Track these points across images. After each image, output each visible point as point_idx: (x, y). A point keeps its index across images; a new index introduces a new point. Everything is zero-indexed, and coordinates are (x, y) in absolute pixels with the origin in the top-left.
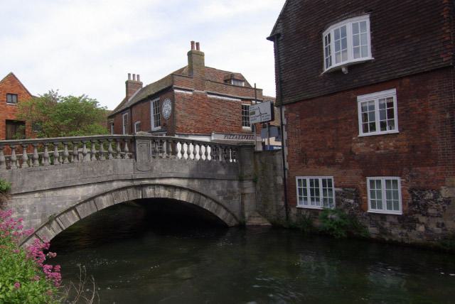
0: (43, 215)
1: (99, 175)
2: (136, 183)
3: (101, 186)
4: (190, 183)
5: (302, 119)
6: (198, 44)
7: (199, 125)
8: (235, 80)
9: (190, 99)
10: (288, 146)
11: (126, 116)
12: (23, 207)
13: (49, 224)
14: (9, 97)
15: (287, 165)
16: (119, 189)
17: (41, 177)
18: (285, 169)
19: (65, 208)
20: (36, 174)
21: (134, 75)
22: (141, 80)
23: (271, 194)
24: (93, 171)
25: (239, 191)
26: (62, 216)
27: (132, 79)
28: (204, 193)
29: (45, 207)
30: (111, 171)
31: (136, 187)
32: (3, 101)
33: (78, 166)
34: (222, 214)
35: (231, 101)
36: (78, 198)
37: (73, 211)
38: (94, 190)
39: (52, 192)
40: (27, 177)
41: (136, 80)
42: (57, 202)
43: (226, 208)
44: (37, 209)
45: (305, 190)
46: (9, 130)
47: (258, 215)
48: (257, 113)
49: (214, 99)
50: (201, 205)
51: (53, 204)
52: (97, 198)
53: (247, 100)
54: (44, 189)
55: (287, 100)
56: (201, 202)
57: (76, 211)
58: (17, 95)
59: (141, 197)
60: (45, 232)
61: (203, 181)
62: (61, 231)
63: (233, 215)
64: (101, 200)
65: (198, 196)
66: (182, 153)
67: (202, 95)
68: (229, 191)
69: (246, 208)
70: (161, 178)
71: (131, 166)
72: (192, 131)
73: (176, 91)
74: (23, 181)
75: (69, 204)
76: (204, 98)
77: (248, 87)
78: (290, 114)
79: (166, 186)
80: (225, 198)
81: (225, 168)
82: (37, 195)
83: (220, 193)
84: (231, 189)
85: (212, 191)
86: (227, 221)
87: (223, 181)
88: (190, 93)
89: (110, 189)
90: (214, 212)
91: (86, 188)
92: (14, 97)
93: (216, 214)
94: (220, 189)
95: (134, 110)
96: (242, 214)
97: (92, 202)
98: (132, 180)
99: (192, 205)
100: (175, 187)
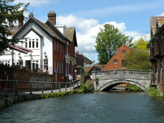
2: (120, 79)
13: (104, 85)
19: (107, 83)
31: (120, 80)
58: (125, 51)
71: (119, 76)
83: (143, 83)
84: (146, 82)
92: (125, 52)
100: (129, 81)
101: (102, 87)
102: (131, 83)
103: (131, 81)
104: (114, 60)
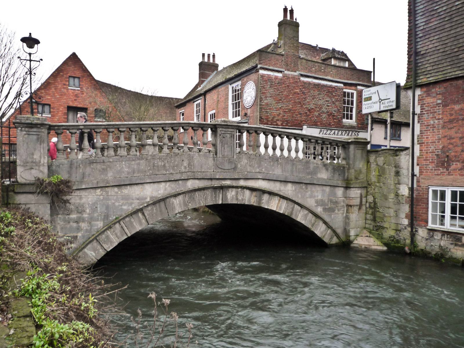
0: (107, 216)
1: (172, 171)
2: (216, 184)
3: (173, 185)
4: (282, 189)
5: (445, 106)
6: (292, 11)
7: (287, 116)
8: (336, 58)
9: (281, 82)
10: (421, 144)
11: (198, 105)
12: (83, 206)
14: (71, 80)
16: (195, 190)
17: (104, 171)
18: (413, 175)
20: (99, 166)
21: (209, 55)
22: (216, 62)
23: (389, 208)
24: (164, 166)
25: (344, 201)
26: (127, 219)
27: (206, 60)
28: (299, 201)
29: (107, 207)
30: (185, 168)
31: (215, 188)
32: (65, 84)
33: (147, 159)
34: (320, 230)
35: (331, 87)
36: (146, 198)
37: (140, 214)
38: (165, 189)
39: (116, 189)
40: (88, 170)
41: (211, 61)
42: (122, 202)
43: (325, 223)
44: (99, 209)
45: (443, 206)
47: (368, 234)
48: (375, 98)
49: (309, 83)
50: (293, 217)
51: (117, 204)
52: (168, 200)
53: (351, 85)
54: (108, 185)
55: (423, 80)
56: (294, 212)
57: (143, 214)
58: (79, 78)
59: (220, 202)
60: (108, 237)
61: (298, 186)
62: (125, 237)
63: (334, 231)
64: (173, 203)
65: (291, 205)
66: (266, 147)
67: (294, 77)
68: (331, 201)
69: (352, 224)
70: (246, 179)
72: (279, 123)
73: (261, 72)
74: (84, 174)
75: (136, 205)
76: (296, 81)
77: (352, 68)
78: (430, 100)
80: (325, 210)
81: (327, 170)
82: (98, 191)
83: (319, 203)
85: (309, 200)
86: (326, 240)
87: (324, 188)
88: (280, 75)
89: (183, 189)
90: (309, 226)
91: (156, 185)
93: (312, 229)
94: (320, 197)
95: (208, 96)
96: (346, 232)
97: (162, 204)
98: (211, 179)
99: (283, 215)
100: (264, 192)
101: (96, 238)
103: (271, 194)
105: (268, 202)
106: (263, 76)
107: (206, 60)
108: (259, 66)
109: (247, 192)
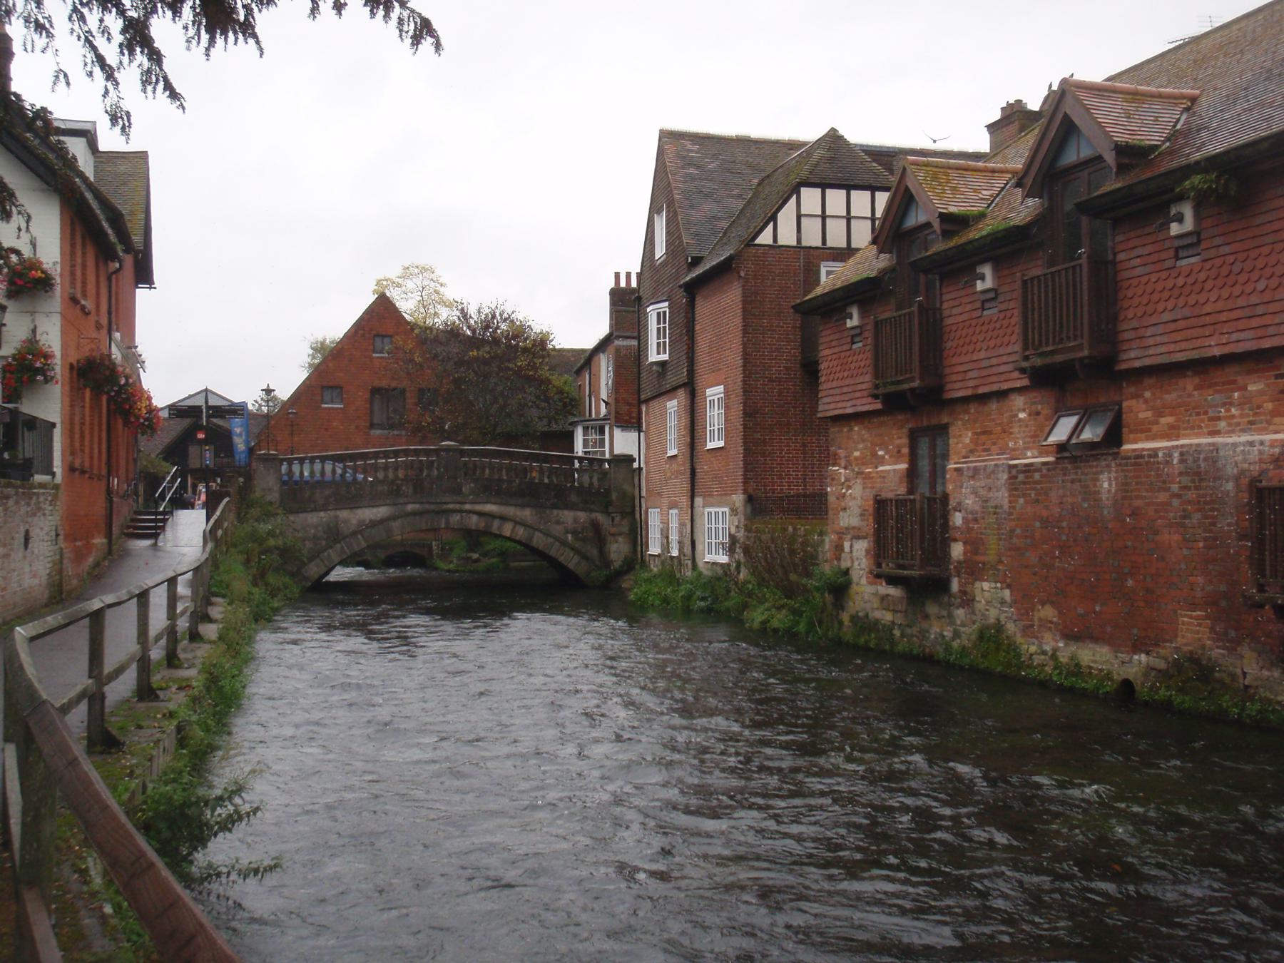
14: (378, 340)
15: (644, 494)
18: (640, 497)
21: (628, 275)
27: (623, 284)
37: (360, 536)
46: (376, 407)
60: (329, 555)
73: (619, 343)
79: (480, 514)
92: (386, 340)
102: (507, 530)
103: (503, 518)
104: (323, 387)
105: (499, 528)
106: (618, 350)
107: (623, 284)
108: (615, 334)
109: (475, 518)
